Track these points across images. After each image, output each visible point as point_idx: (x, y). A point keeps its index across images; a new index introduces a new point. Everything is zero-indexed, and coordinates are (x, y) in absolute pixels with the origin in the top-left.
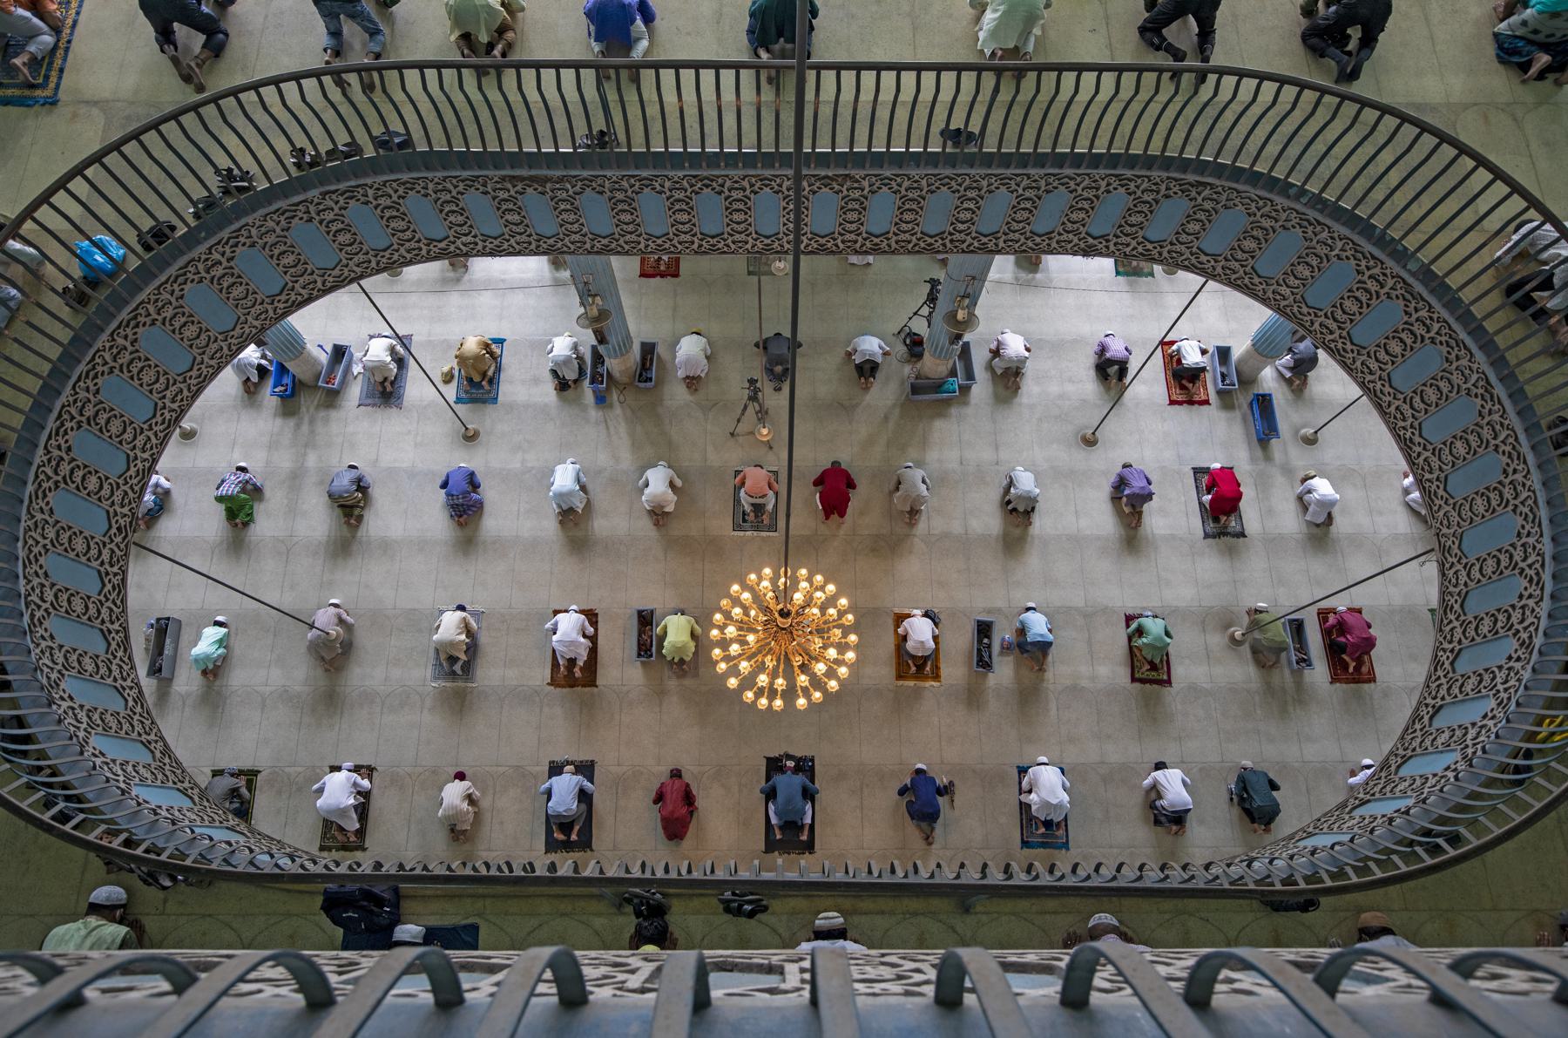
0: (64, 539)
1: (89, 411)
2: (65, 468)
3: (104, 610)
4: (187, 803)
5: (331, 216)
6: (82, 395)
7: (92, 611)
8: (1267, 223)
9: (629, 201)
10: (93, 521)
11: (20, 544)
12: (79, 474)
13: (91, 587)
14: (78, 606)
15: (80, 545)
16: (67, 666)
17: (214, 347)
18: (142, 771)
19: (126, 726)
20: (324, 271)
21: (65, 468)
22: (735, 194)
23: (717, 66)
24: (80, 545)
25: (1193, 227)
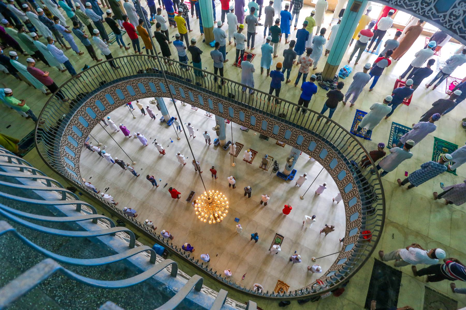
0: (85, 116)
1: (102, 98)
2: (92, 105)
3: (85, 131)
4: (74, 166)
5: (156, 83)
6: (101, 94)
7: (83, 129)
8: (331, 155)
9: (206, 99)
10: (91, 114)
11: (76, 112)
12: (94, 107)
13: (85, 125)
14: (81, 127)
15: (88, 118)
16: (71, 134)
17: (129, 97)
18: (70, 156)
19: (74, 149)
20: (153, 93)
21: (92, 105)
22: (225, 105)
23: (236, 83)
24: (88, 118)
25: (317, 150)
